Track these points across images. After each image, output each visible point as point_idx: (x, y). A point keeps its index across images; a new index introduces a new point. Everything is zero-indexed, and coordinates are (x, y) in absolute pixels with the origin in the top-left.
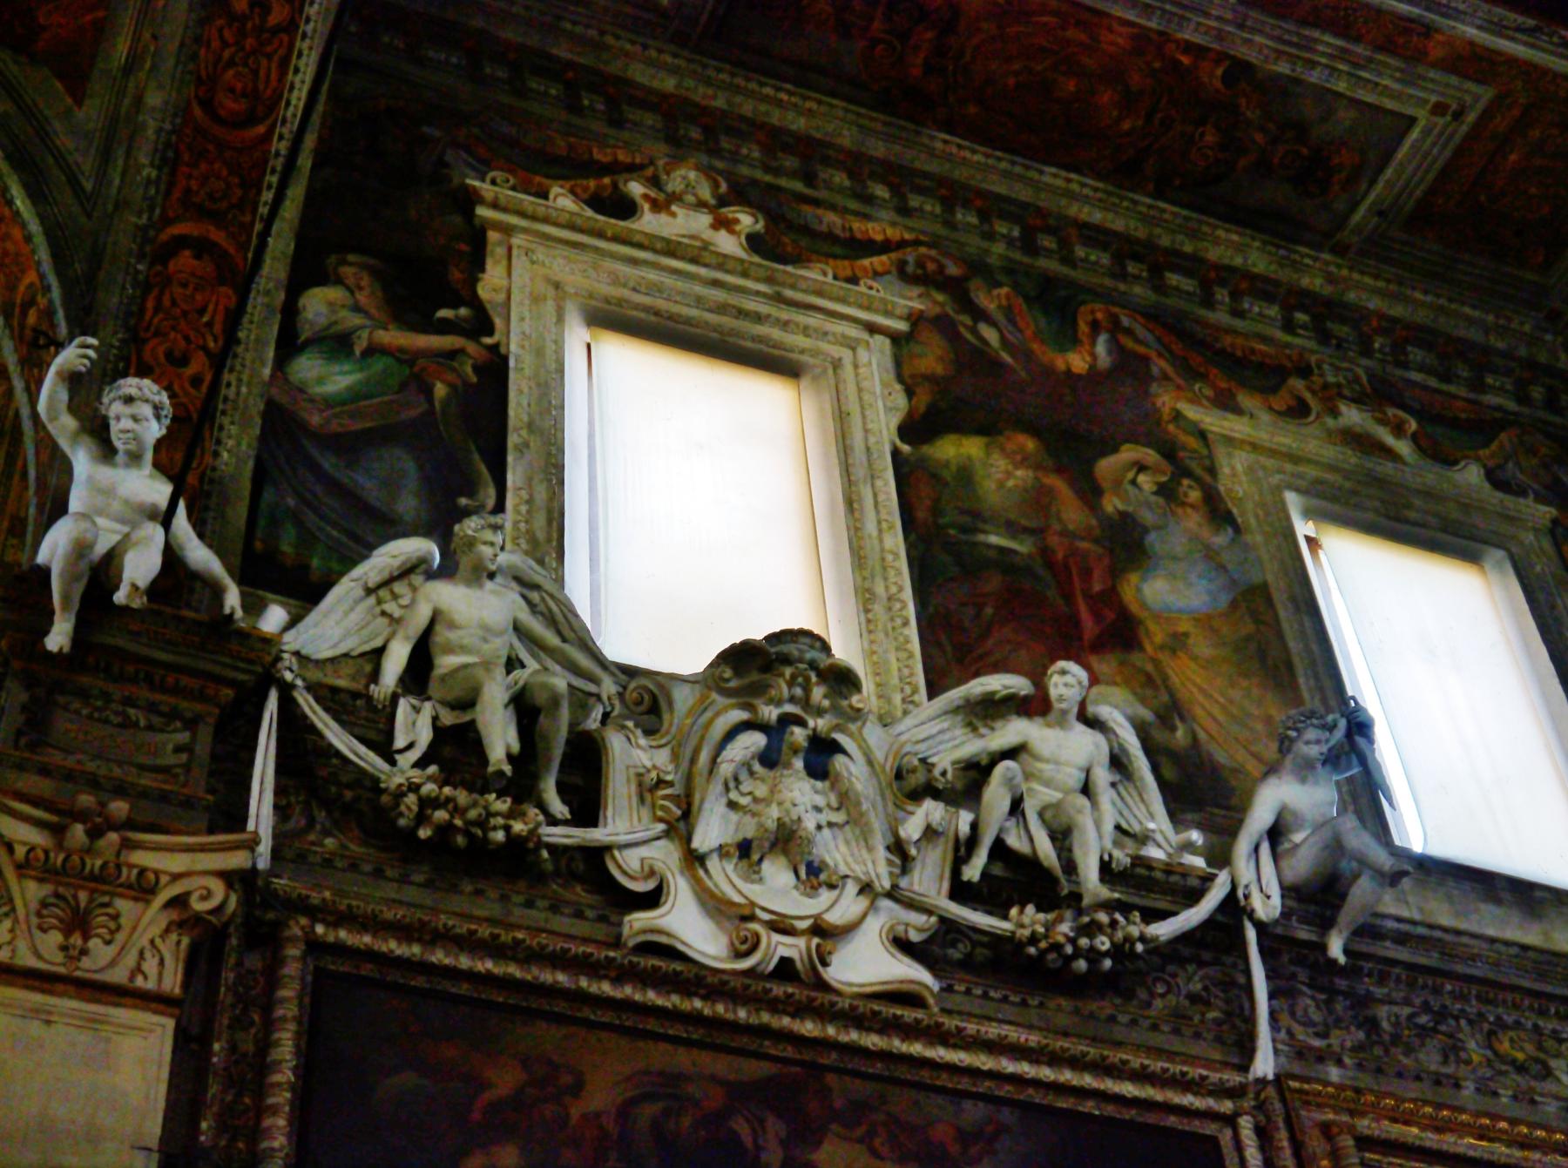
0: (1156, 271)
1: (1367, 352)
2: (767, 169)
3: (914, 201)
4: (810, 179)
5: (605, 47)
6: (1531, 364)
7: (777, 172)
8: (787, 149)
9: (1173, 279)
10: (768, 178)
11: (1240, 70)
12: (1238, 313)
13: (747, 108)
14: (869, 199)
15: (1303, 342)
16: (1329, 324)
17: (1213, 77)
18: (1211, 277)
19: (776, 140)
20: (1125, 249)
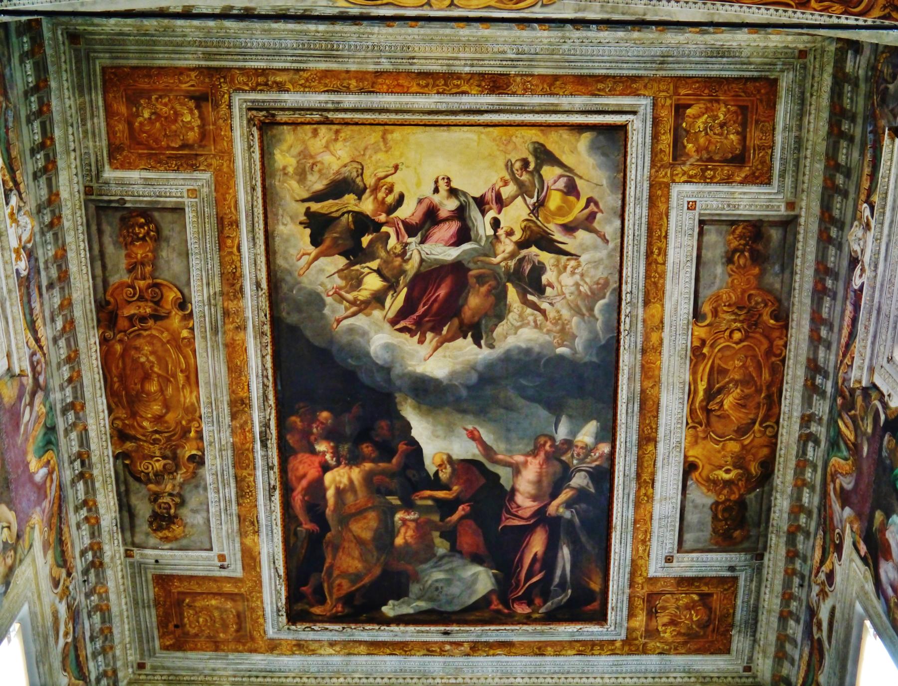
0: (81, 476)
1: (87, 596)
2: (46, 262)
3: (62, 343)
4: (51, 286)
5: (68, 154)
6: (115, 672)
7: (47, 268)
8: (59, 267)
9: (81, 486)
10: (42, 266)
11: (198, 461)
12: (78, 527)
13: (69, 239)
14: (53, 320)
15: (79, 564)
16: (92, 571)
17: (189, 450)
18: (89, 504)
19: (61, 259)
20: (83, 457)
